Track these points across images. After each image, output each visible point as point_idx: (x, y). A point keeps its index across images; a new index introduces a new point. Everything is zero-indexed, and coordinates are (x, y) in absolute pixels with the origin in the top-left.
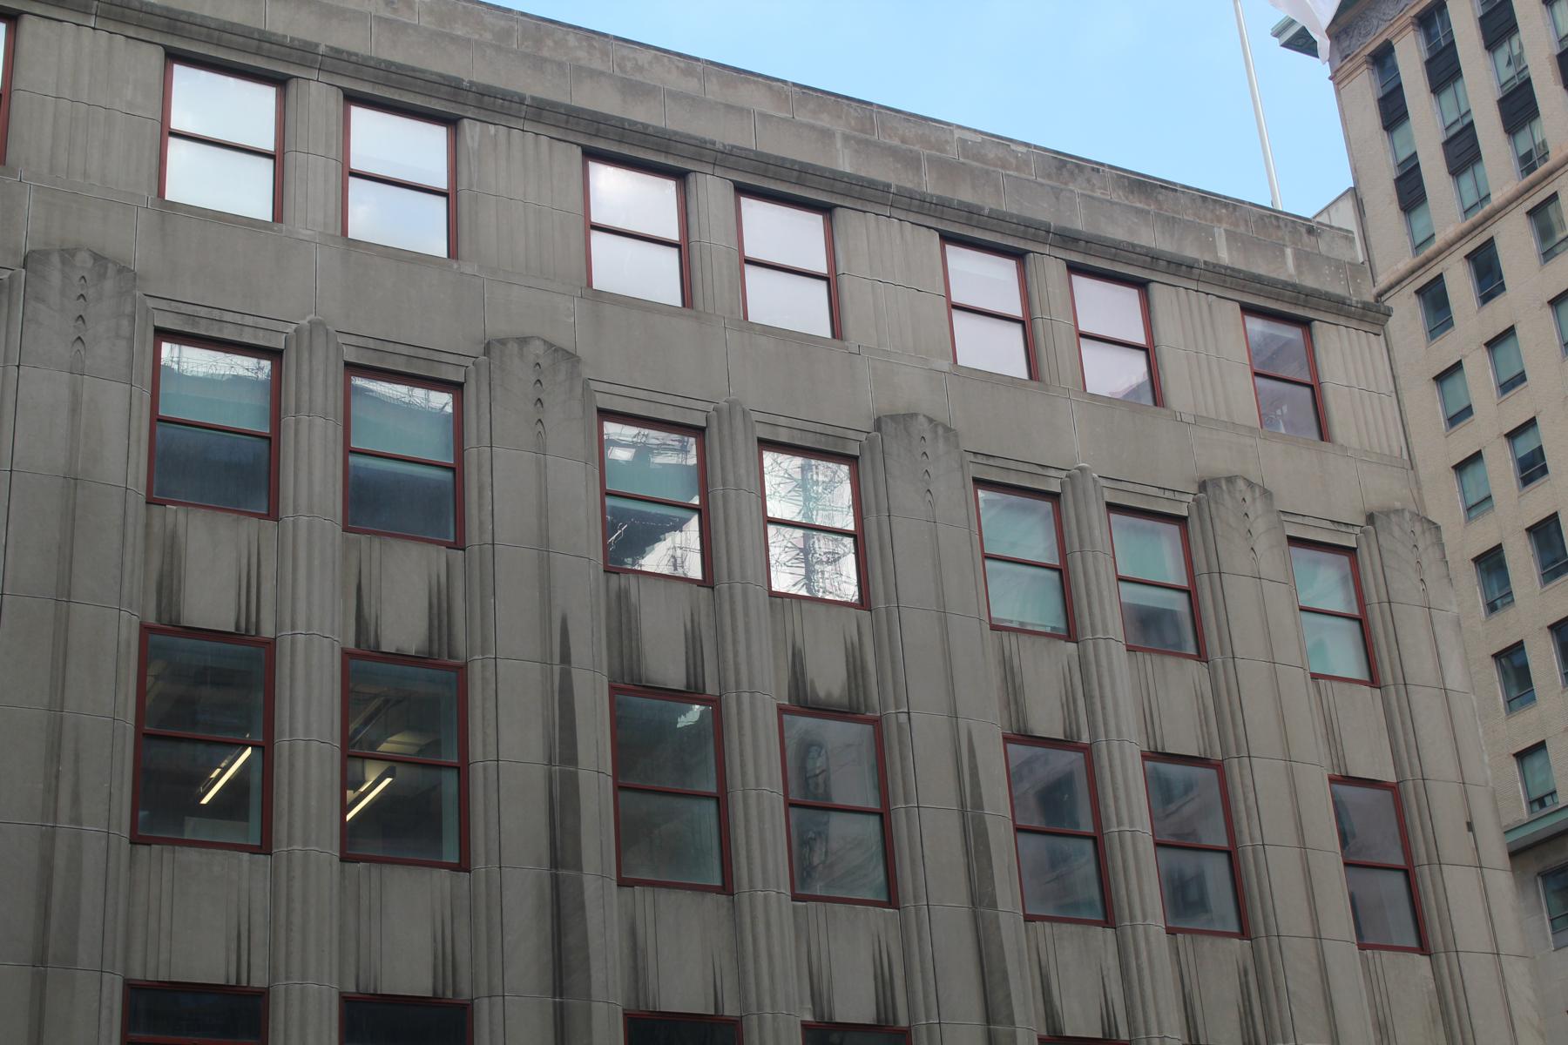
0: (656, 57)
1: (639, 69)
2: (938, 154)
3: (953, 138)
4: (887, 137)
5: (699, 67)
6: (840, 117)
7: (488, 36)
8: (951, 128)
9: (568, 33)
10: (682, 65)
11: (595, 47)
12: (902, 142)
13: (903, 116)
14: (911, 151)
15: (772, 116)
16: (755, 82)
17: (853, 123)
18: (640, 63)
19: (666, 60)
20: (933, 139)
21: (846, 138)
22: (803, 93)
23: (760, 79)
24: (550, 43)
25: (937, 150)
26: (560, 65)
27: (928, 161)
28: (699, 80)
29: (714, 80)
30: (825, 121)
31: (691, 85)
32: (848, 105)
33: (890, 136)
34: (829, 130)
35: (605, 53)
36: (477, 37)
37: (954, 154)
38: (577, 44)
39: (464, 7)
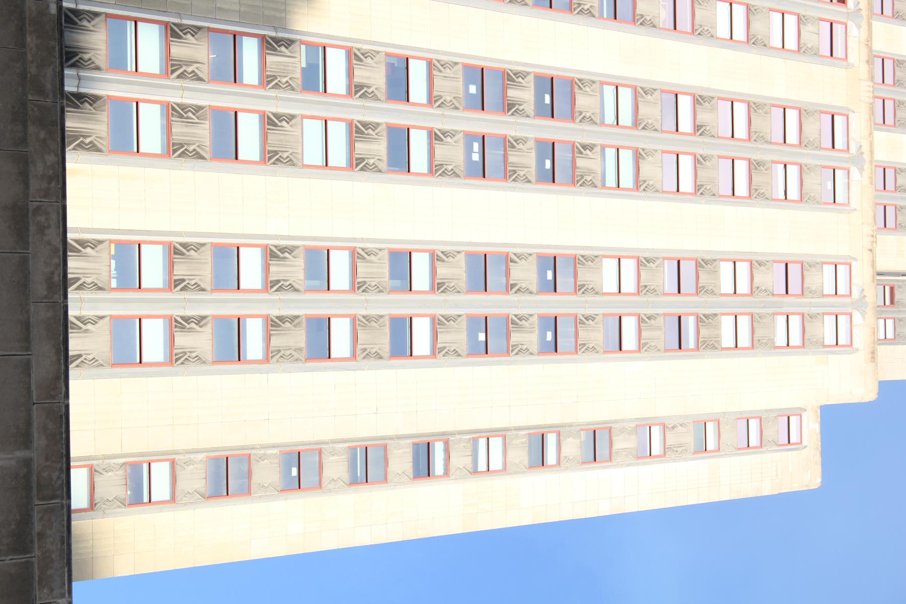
0: (57, 250)
1: (42, 230)
2: (37, 578)
3: (56, 598)
4: (40, 515)
5: (58, 298)
6: (47, 459)
7: (33, 70)
8: (67, 595)
9: (56, 155)
10: (56, 278)
11: (49, 183)
12: (39, 534)
13: (65, 535)
14: (32, 542)
15: (29, 376)
16: (59, 360)
17: (45, 474)
18: (47, 231)
19: (56, 260)
20: (50, 572)
21: (28, 463)
22: (61, 416)
23: (63, 367)
24: (42, 135)
25: (40, 578)
26: (24, 141)
27: (26, 562)
28: (46, 297)
29: (49, 314)
30: (39, 440)
31: (39, 288)
32: (61, 469)
33: (41, 519)
34: (31, 442)
35: (47, 193)
36: (29, 57)
37: (40, 598)
38: (49, 164)
39: (54, 48)
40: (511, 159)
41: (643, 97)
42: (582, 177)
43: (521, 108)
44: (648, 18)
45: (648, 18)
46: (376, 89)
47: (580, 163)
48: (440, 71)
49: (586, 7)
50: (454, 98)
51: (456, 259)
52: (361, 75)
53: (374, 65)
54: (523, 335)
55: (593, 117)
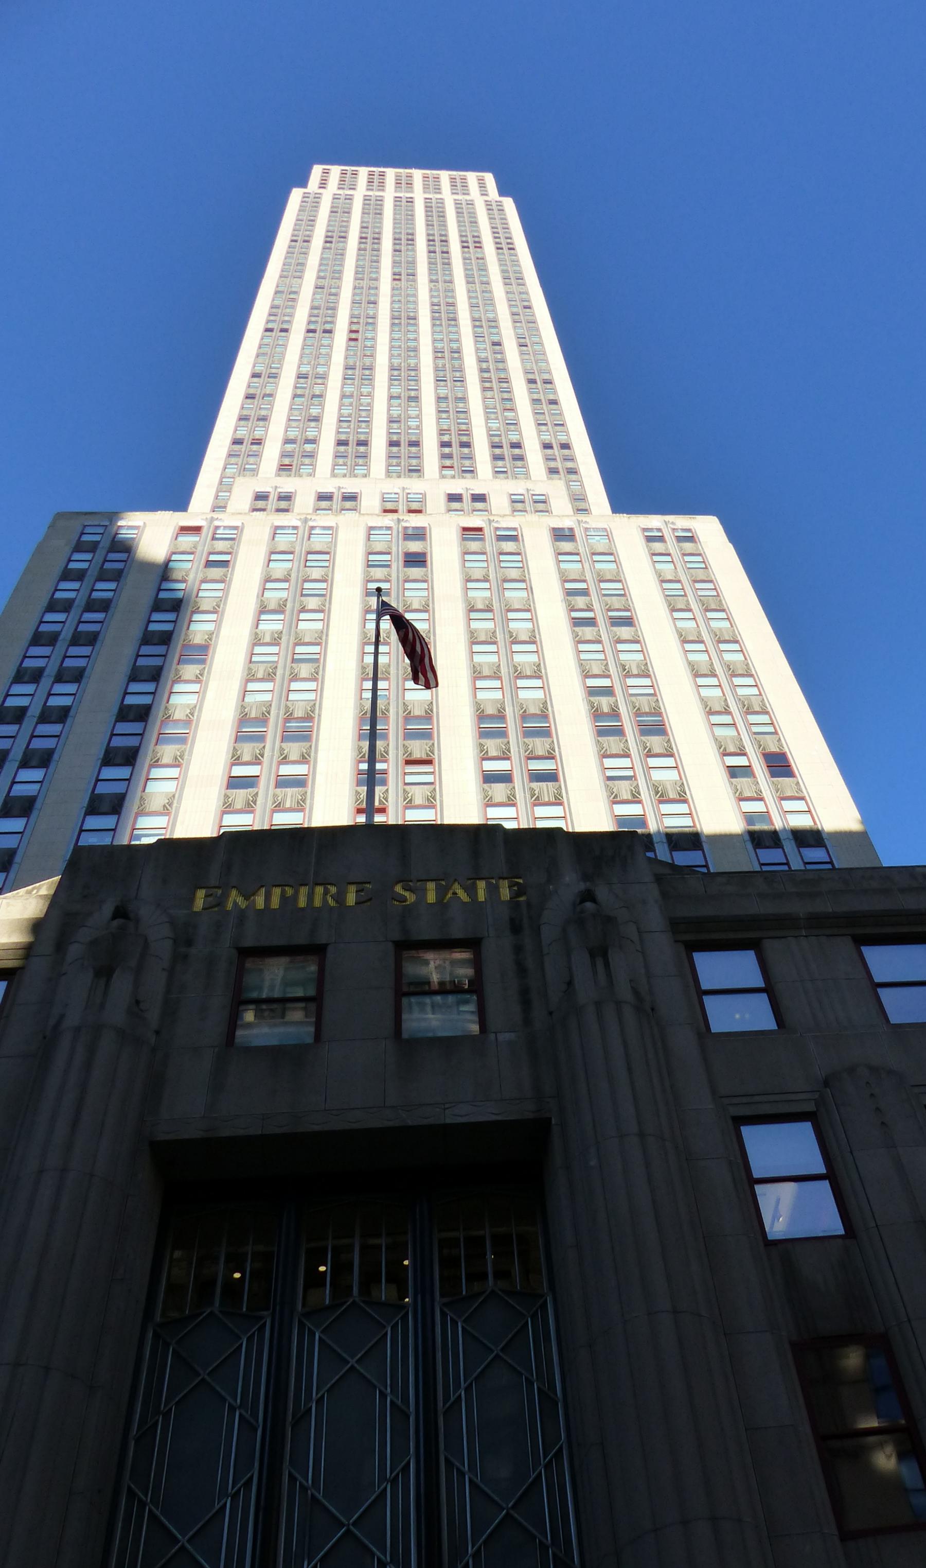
40: (647, 710)
41: (581, 637)
42: (643, 671)
43: (613, 705)
44: (530, 634)
45: (530, 634)
46: (631, 786)
47: (635, 672)
48: (606, 750)
49: (536, 668)
50: (621, 742)
51: (721, 740)
52: (626, 796)
53: (617, 787)
54: (753, 703)
55: (604, 664)
